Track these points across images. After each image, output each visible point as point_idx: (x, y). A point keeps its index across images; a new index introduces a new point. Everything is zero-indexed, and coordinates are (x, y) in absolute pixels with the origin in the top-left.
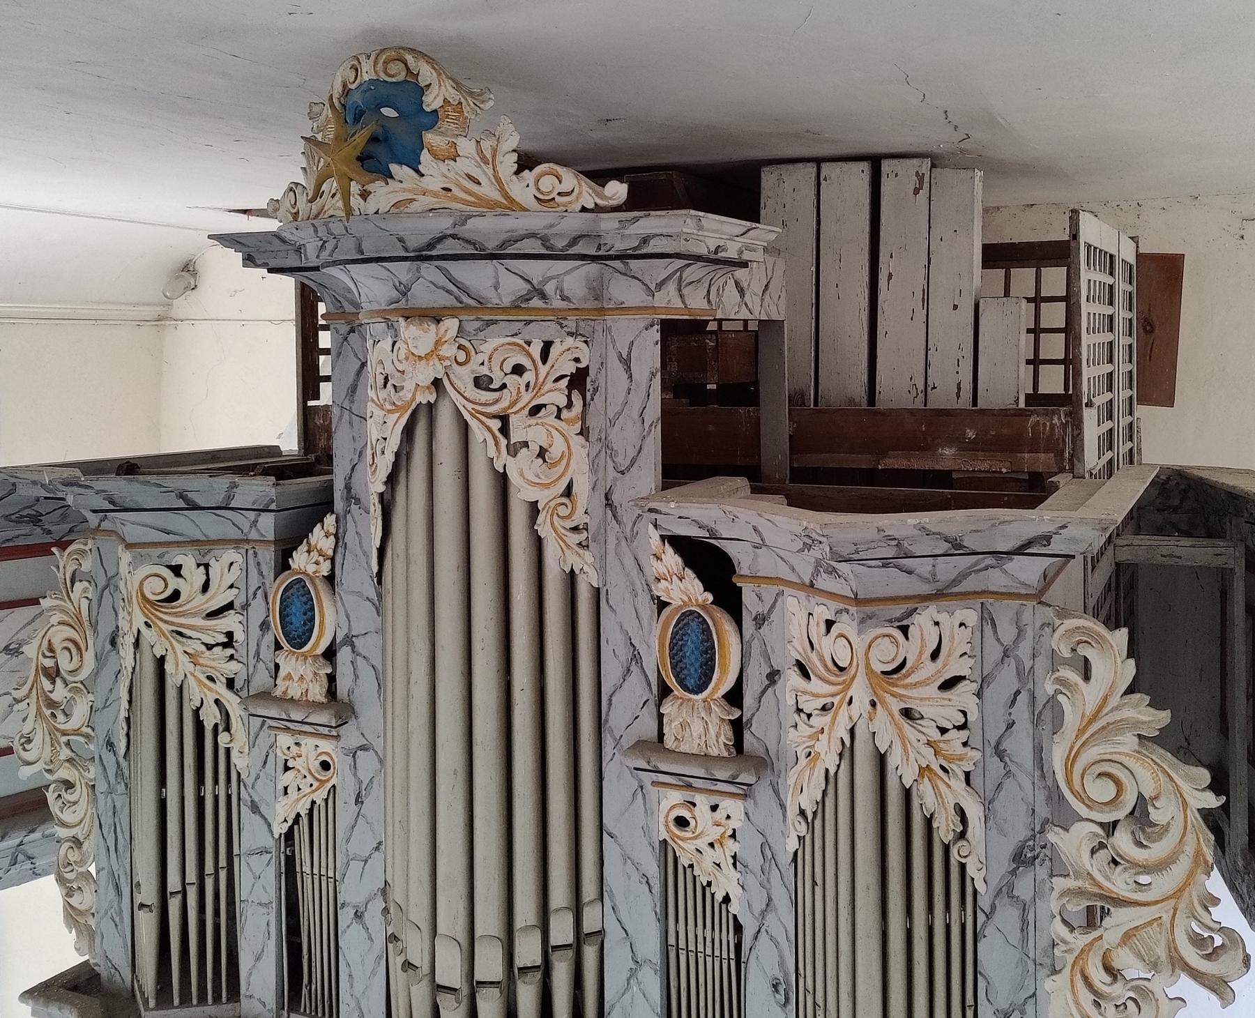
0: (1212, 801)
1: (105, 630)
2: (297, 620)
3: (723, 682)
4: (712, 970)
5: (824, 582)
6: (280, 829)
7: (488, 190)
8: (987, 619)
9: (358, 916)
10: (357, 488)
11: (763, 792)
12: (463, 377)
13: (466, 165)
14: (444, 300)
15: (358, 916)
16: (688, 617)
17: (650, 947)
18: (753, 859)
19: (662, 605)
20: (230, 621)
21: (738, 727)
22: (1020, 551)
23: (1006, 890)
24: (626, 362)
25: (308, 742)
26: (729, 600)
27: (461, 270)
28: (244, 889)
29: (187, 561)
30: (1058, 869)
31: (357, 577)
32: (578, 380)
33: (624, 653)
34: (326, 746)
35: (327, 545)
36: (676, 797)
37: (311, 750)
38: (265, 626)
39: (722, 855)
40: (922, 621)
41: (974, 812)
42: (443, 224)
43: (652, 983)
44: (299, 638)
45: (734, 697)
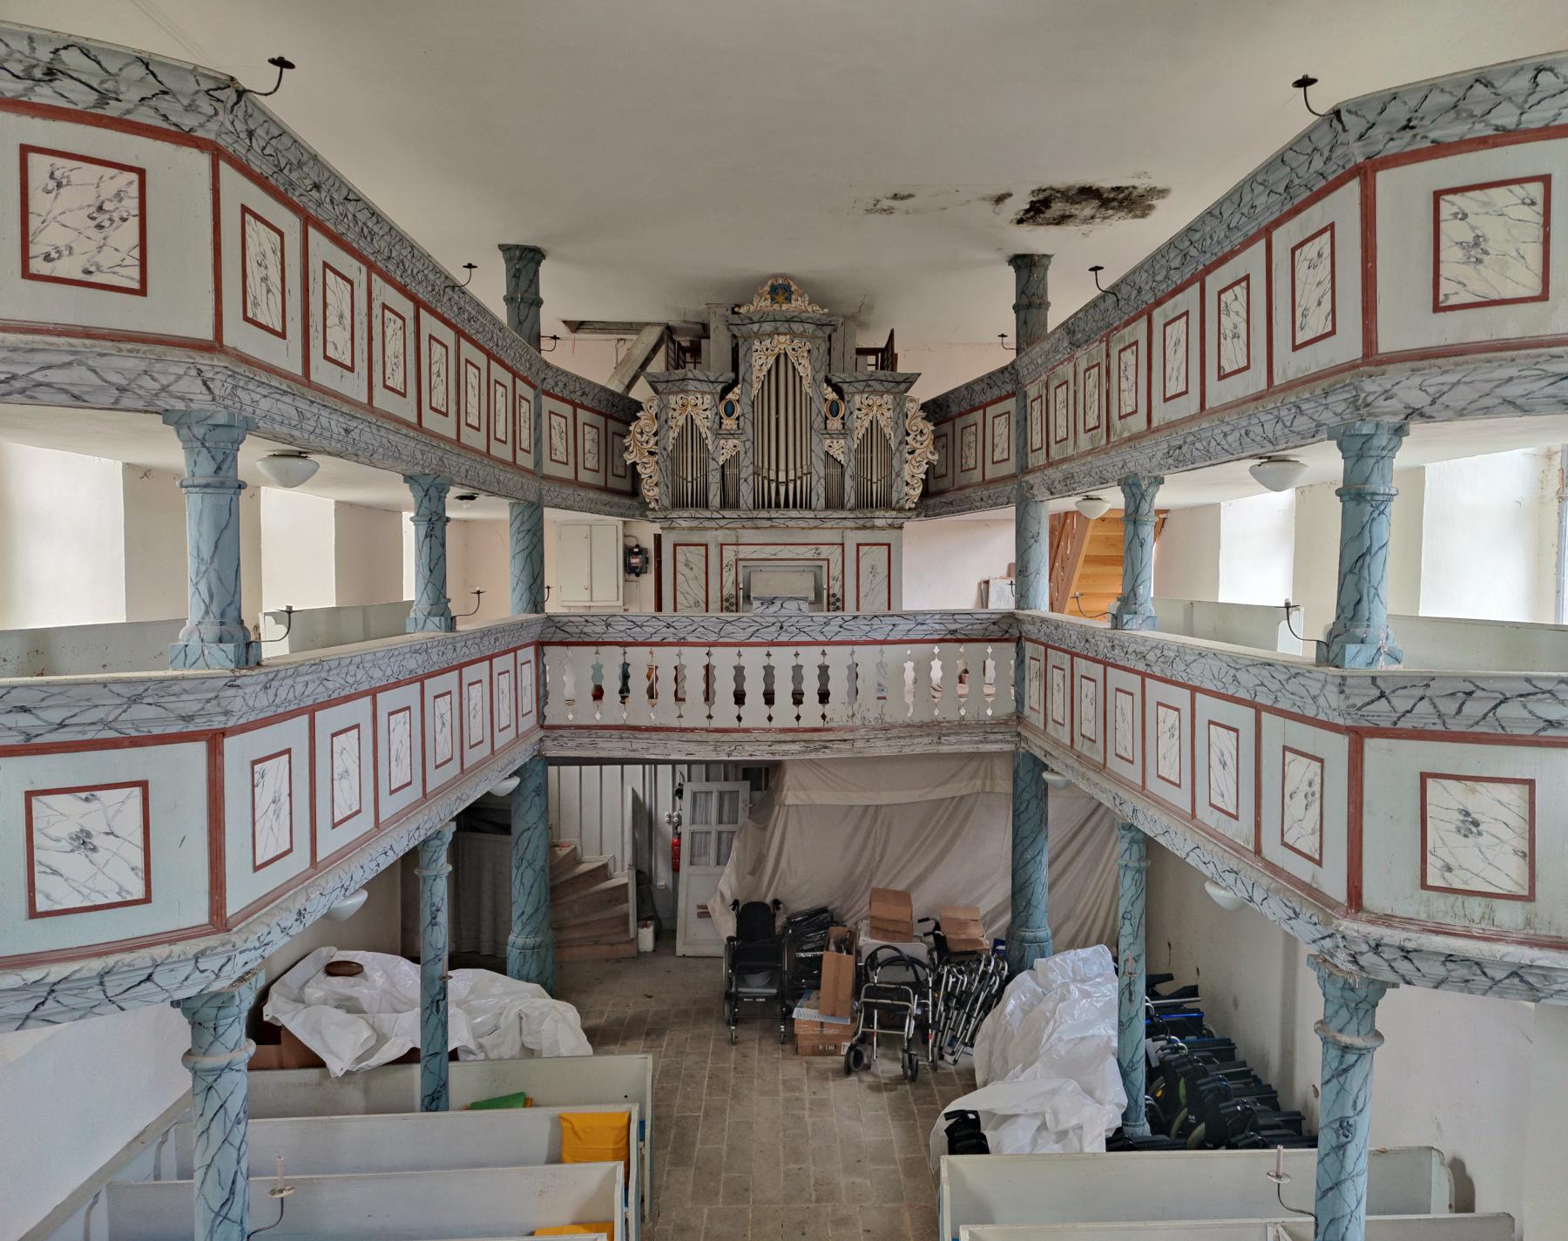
0: (933, 428)
2: (729, 409)
3: (841, 415)
4: (836, 478)
5: (867, 389)
6: (721, 463)
7: (803, 308)
8: (895, 398)
9: (746, 480)
10: (747, 377)
11: (849, 437)
12: (790, 348)
13: (800, 302)
14: (786, 331)
15: (746, 480)
16: (833, 402)
17: (822, 474)
19: (826, 400)
20: (708, 413)
21: (843, 424)
22: (904, 382)
23: (897, 449)
24: (818, 349)
25: (730, 441)
26: (842, 398)
27: (792, 325)
28: (710, 479)
29: (699, 396)
30: (907, 444)
31: (745, 400)
32: (809, 351)
35: (739, 392)
36: (829, 441)
37: (731, 443)
38: (716, 414)
40: (885, 396)
43: (823, 481)
44: (729, 415)
45: (843, 418)
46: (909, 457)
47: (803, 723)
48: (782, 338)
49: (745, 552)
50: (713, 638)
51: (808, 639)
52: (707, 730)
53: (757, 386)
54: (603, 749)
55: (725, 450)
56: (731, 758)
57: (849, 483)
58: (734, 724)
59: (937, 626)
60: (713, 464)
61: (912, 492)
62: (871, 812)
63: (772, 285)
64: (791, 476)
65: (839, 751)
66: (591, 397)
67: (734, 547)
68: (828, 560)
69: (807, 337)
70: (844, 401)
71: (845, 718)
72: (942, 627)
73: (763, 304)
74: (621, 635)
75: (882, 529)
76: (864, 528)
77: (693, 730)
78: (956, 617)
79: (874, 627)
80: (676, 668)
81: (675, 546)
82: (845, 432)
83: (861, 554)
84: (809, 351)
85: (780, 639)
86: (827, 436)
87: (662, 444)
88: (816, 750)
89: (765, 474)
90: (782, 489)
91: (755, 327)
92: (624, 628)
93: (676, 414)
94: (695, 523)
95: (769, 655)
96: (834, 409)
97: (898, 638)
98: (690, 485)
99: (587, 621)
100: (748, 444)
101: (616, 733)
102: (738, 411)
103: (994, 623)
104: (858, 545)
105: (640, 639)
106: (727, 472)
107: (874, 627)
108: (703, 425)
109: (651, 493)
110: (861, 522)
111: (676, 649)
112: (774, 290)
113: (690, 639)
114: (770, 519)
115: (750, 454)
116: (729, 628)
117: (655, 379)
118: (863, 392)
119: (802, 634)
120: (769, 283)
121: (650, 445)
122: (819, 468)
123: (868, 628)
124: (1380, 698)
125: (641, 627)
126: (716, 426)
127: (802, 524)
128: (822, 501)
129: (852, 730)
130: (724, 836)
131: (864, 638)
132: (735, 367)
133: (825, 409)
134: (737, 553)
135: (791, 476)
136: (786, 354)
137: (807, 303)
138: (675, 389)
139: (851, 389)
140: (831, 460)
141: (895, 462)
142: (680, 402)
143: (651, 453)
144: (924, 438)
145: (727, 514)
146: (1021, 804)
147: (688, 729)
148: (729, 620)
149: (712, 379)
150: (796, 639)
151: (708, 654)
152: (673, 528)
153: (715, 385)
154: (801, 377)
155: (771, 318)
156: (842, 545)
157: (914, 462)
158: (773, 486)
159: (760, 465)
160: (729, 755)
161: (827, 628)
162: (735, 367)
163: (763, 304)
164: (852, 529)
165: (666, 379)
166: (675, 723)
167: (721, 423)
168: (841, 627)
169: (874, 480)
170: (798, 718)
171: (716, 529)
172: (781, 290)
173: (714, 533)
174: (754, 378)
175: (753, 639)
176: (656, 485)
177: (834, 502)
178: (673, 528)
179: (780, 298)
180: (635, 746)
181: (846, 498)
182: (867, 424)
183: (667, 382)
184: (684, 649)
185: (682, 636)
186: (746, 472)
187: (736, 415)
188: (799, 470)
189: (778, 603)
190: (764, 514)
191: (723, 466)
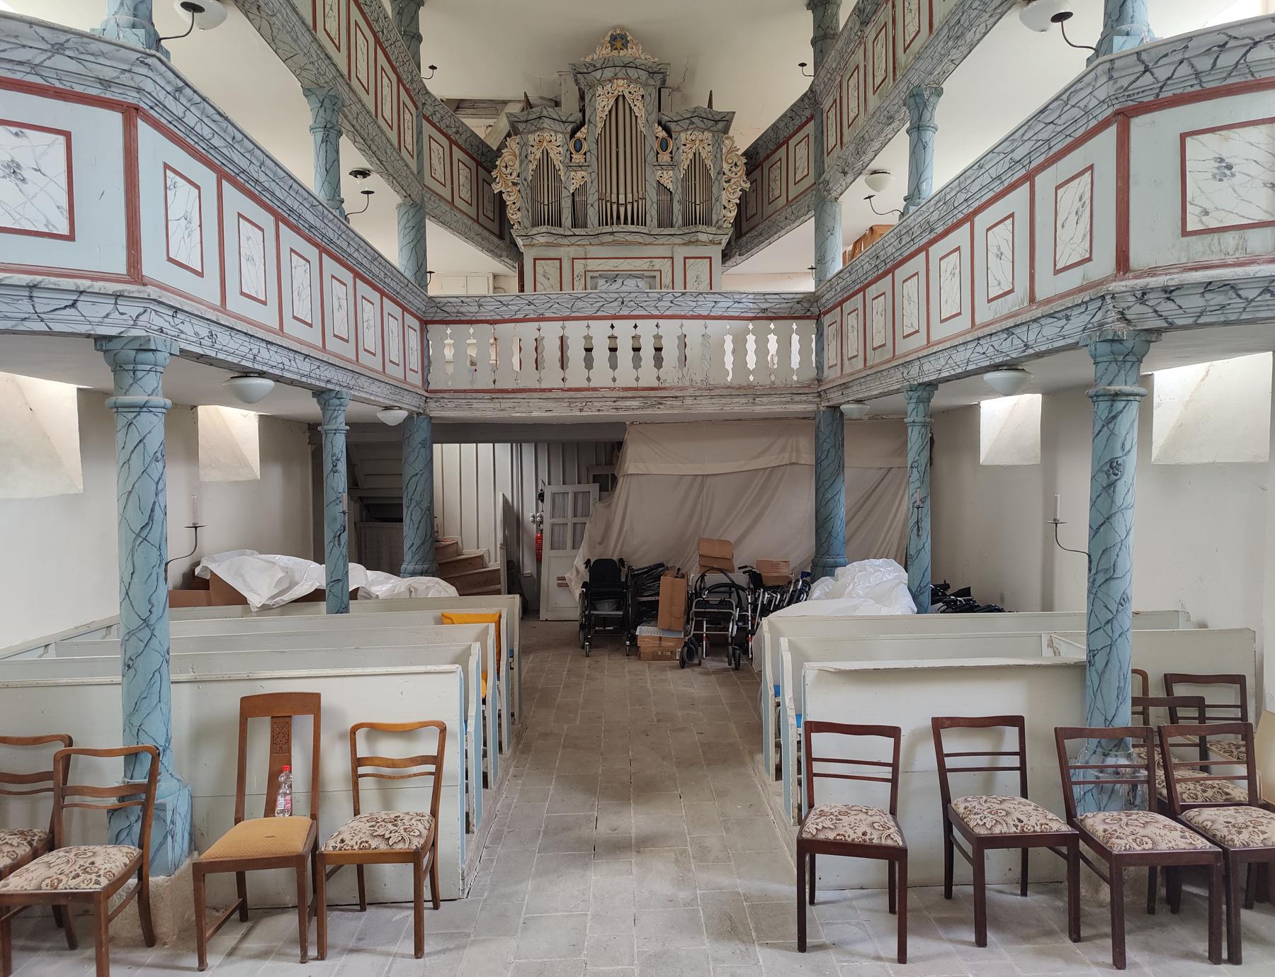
0: (746, 161)
1: (524, 155)
2: (578, 147)
5: (691, 127)
6: (571, 192)
8: (714, 136)
9: (592, 205)
13: (634, 50)
16: (663, 139)
17: (655, 200)
18: (675, 181)
19: (657, 138)
20: (560, 149)
21: (672, 158)
23: (716, 179)
25: (579, 173)
29: (553, 134)
30: (724, 174)
33: (650, 147)
34: (583, 173)
35: (586, 131)
36: (660, 172)
37: (580, 174)
38: (567, 150)
39: (669, 181)
40: (706, 133)
41: (712, 166)
42: (632, 60)
43: (655, 205)
44: (578, 151)
45: (671, 153)
46: (726, 185)
47: (642, 384)
48: (621, 82)
49: (592, 265)
50: (566, 313)
51: (645, 313)
52: (562, 390)
53: (600, 125)
54: (477, 409)
55: (574, 180)
56: (583, 414)
57: (677, 207)
58: (585, 384)
59: (751, 305)
60: (565, 193)
61: (728, 214)
62: (699, 479)
63: (612, 35)
64: (630, 199)
65: (672, 407)
66: (464, 137)
67: (583, 261)
68: (661, 271)
69: (641, 84)
70: (671, 137)
71: (676, 380)
72: (755, 306)
73: (604, 52)
74: (491, 314)
75: (704, 244)
76: (690, 243)
77: (550, 390)
78: (766, 296)
79: (699, 303)
80: (536, 340)
81: (535, 259)
82: (673, 165)
83: (687, 265)
84: (643, 96)
85: (622, 313)
86: (659, 168)
87: (522, 176)
88: (652, 406)
89: (608, 198)
90: (622, 209)
91: (598, 74)
92: (494, 307)
93: (534, 150)
94: (551, 239)
95: (612, 327)
96: (664, 145)
97: (719, 313)
98: (546, 207)
99: (462, 302)
100: (594, 175)
101: (488, 396)
102: (585, 147)
103: (798, 303)
104: (685, 258)
105: (506, 317)
106: (577, 199)
107: (699, 303)
108: (557, 157)
109: (514, 217)
110: (687, 238)
111: (536, 324)
112: (614, 38)
113: (547, 315)
114: (612, 233)
115: (595, 183)
116: (579, 304)
117: (516, 119)
118: (687, 129)
119: (640, 308)
120: (610, 34)
121: (513, 177)
122: (652, 194)
123: (694, 304)
124: (1144, 72)
125: (507, 305)
126: (568, 161)
127: (638, 238)
128: (655, 222)
129: (682, 389)
130: (579, 527)
131: (691, 313)
132: (583, 110)
133: (656, 146)
134: (585, 265)
135: (630, 199)
136: (623, 96)
137: (640, 52)
138: (533, 128)
139: (678, 128)
140: (661, 187)
141: (715, 190)
142: (537, 139)
143: (515, 184)
144: (738, 169)
145: (577, 231)
146: (822, 453)
147: (546, 389)
148: (579, 296)
149: (564, 119)
150: (635, 313)
151: (563, 379)
152: (533, 245)
153: (566, 124)
154: (636, 117)
155: (611, 64)
156: (672, 258)
157: (730, 189)
158: (615, 207)
159: (604, 191)
160: (581, 410)
161: (660, 304)
162: (583, 110)
163: (604, 52)
164: (679, 244)
165: (525, 119)
166: (537, 386)
167: (571, 158)
168: (672, 302)
169: (698, 202)
170: (637, 379)
171: (569, 246)
172: (619, 39)
173: (569, 249)
174: (598, 118)
175: (599, 314)
176: (519, 210)
177: (665, 221)
178: (533, 245)
179: (619, 45)
180: (503, 406)
181: (675, 220)
182: (691, 156)
183: (526, 121)
184: (543, 324)
185: (540, 312)
186: (592, 198)
187: (583, 151)
188: (636, 194)
189: (620, 281)
190: (607, 229)
191: (573, 194)
